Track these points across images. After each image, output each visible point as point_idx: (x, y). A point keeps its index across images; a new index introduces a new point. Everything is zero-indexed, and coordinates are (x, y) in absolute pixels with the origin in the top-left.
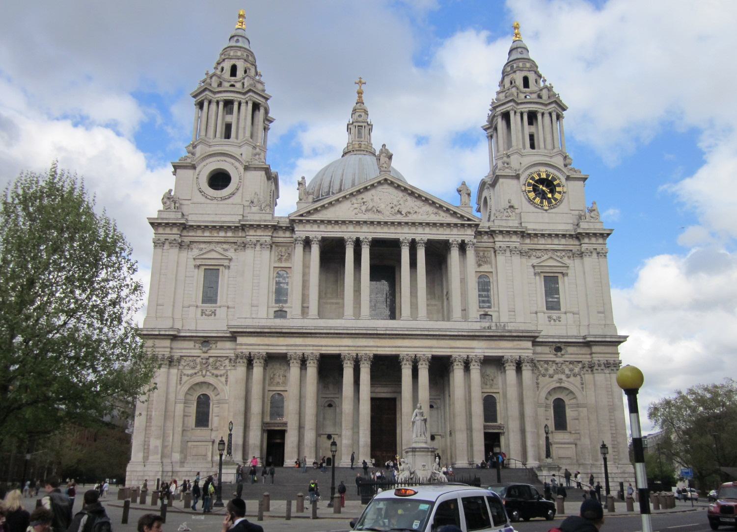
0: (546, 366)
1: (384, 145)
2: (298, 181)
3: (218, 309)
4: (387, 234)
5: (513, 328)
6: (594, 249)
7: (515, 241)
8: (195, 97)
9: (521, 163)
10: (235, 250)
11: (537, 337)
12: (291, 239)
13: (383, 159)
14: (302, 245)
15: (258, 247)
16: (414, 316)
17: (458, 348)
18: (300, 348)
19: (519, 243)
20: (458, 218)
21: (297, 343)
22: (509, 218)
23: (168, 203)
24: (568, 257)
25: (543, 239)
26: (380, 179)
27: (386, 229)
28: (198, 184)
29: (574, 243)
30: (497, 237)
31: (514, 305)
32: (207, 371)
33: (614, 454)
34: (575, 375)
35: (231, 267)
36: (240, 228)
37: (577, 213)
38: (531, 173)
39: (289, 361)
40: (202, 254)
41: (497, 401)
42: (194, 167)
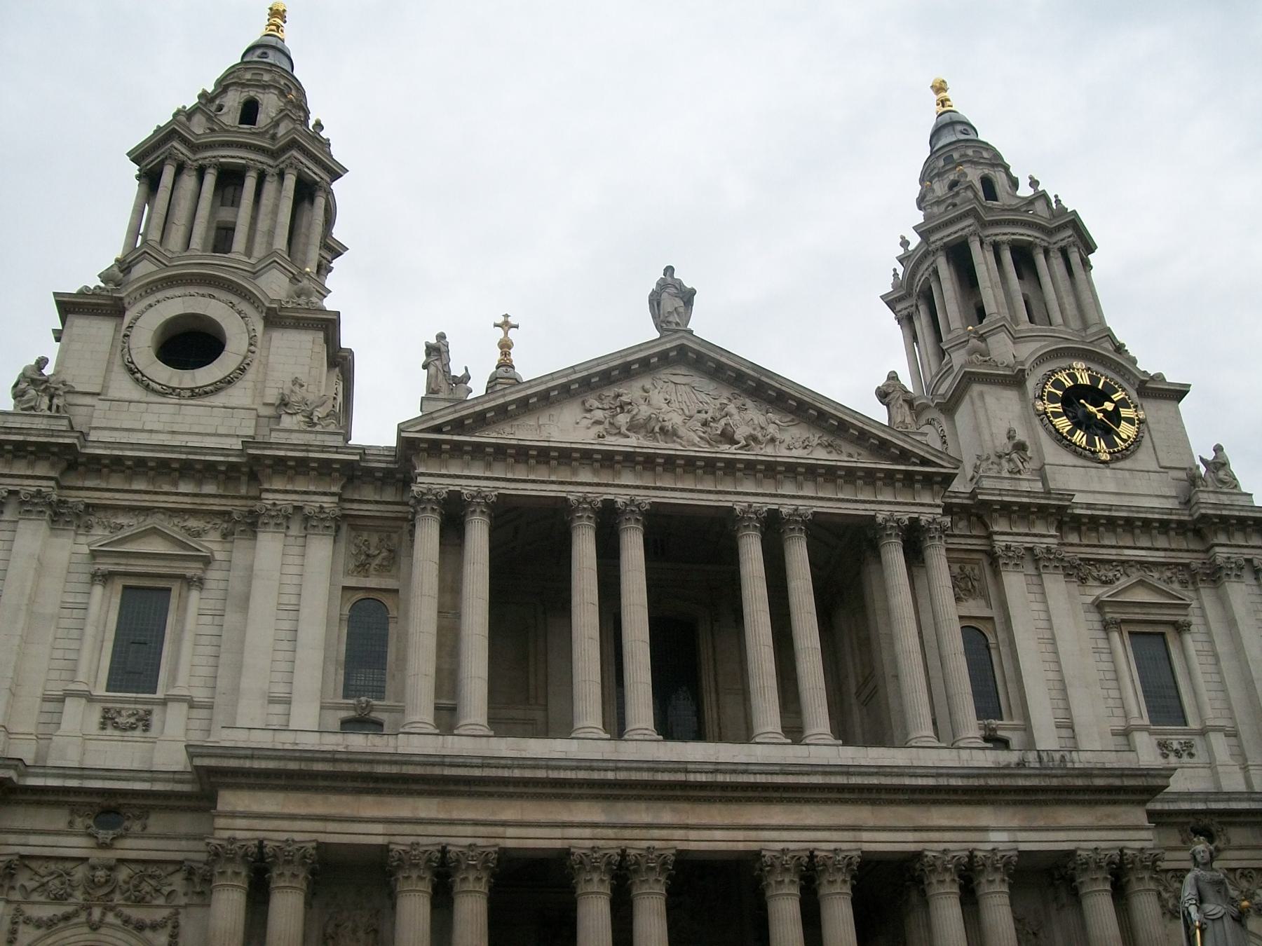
1: (669, 270)
2: (426, 342)
3: (157, 710)
4: (695, 496)
6: (1248, 561)
7: (1045, 537)
10: (225, 536)
11: (1154, 792)
13: (669, 303)
14: (436, 516)
15: (295, 529)
16: (794, 730)
18: (431, 829)
20: (895, 460)
21: (423, 814)
22: (1018, 476)
24: (1181, 582)
26: (668, 346)
28: (126, 350)
29: (1192, 547)
31: (1068, 709)
32: (107, 909)
35: (210, 584)
36: (244, 469)
38: (1054, 372)
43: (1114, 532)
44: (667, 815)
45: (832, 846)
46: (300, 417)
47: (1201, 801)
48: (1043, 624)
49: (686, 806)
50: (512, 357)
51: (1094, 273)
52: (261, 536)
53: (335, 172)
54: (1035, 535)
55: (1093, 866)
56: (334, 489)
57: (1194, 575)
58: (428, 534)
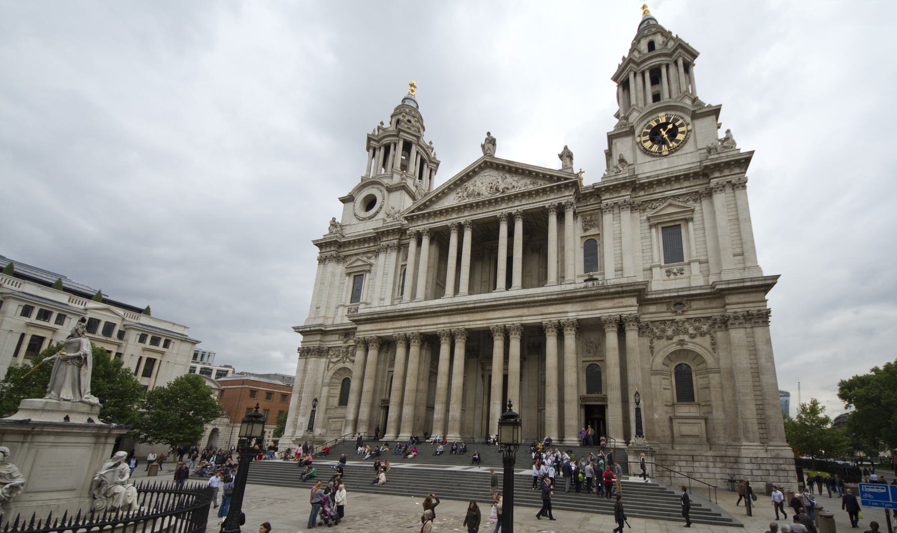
4: (486, 214)
7: (626, 195)
14: (414, 239)
15: (389, 251)
16: (509, 284)
17: (549, 314)
18: (404, 329)
19: (629, 197)
21: (403, 325)
24: (694, 200)
25: (660, 187)
30: (604, 195)
33: (762, 431)
35: (372, 271)
40: (351, 264)
43: (662, 185)
44: (465, 318)
45: (511, 323)
47: (675, 292)
49: (471, 315)
54: (620, 197)
55: (608, 322)
56: (397, 237)
57: (701, 194)
58: (413, 244)
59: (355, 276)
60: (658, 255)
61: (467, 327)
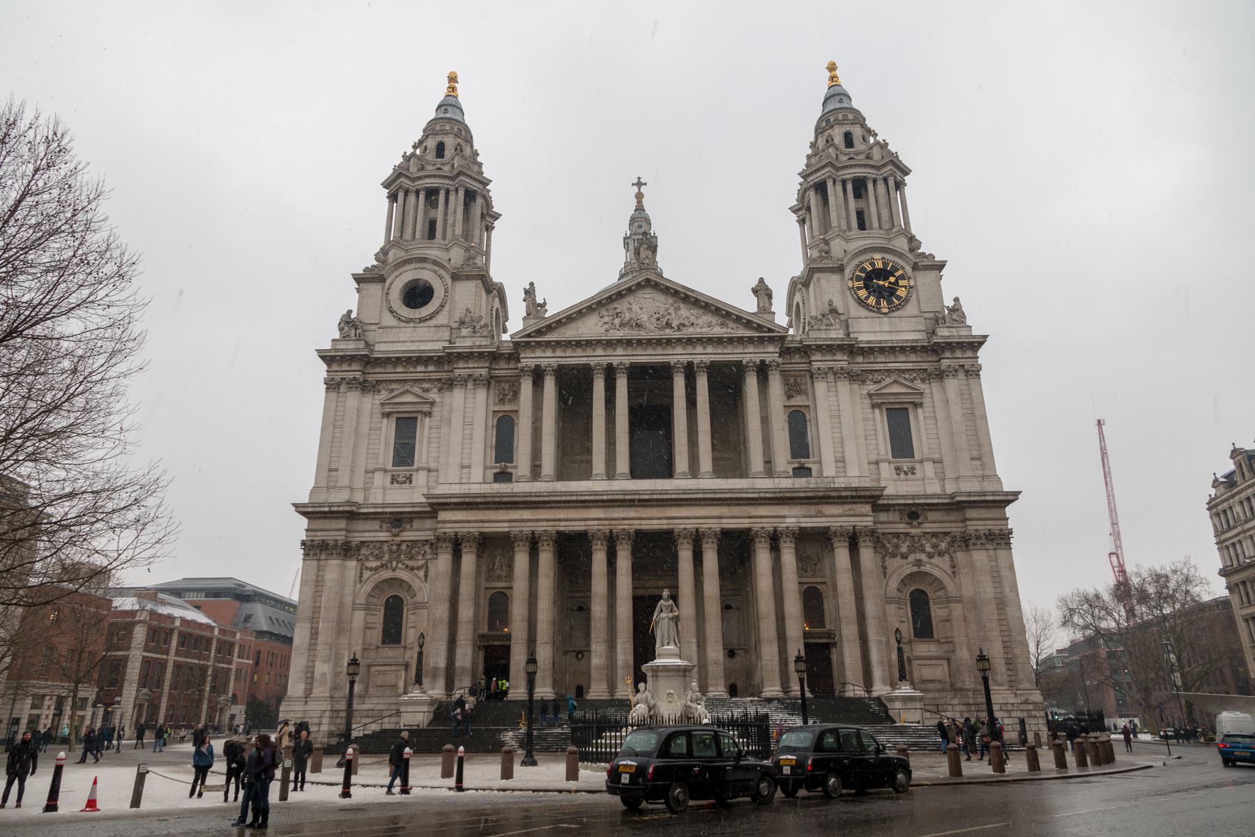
0: (896, 540)
5: (843, 486)
6: (960, 366)
7: (841, 361)
8: (385, 187)
9: (845, 251)
10: (439, 390)
11: (879, 497)
12: (516, 371)
14: (531, 378)
15: (470, 385)
18: (528, 524)
21: (525, 517)
22: (831, 328)
23: (346, 329)
24: (921, 379)
26: (640, 280)
27: (650, 351)
28: (388, 301)
29: (930, 359)
30: (814, 354)
33: (1009, 673)
34: (941, 554)
35: (434, 414)
37: (931, 315)
38: (861, 263)
39: (513, 543)
41: (824, 595)
42: (382, 279)
44: (632, 513)
46: (470, 329)
48: (836, 408)
49: (640, 509)
50: (643, 203)
51: (907, 190)
52: (454, 390)
53: (486, 183)
56: (486, 365)
58: (526, 387)
59: (397, 418)
60: (883, 446)
61: (637, 527)
